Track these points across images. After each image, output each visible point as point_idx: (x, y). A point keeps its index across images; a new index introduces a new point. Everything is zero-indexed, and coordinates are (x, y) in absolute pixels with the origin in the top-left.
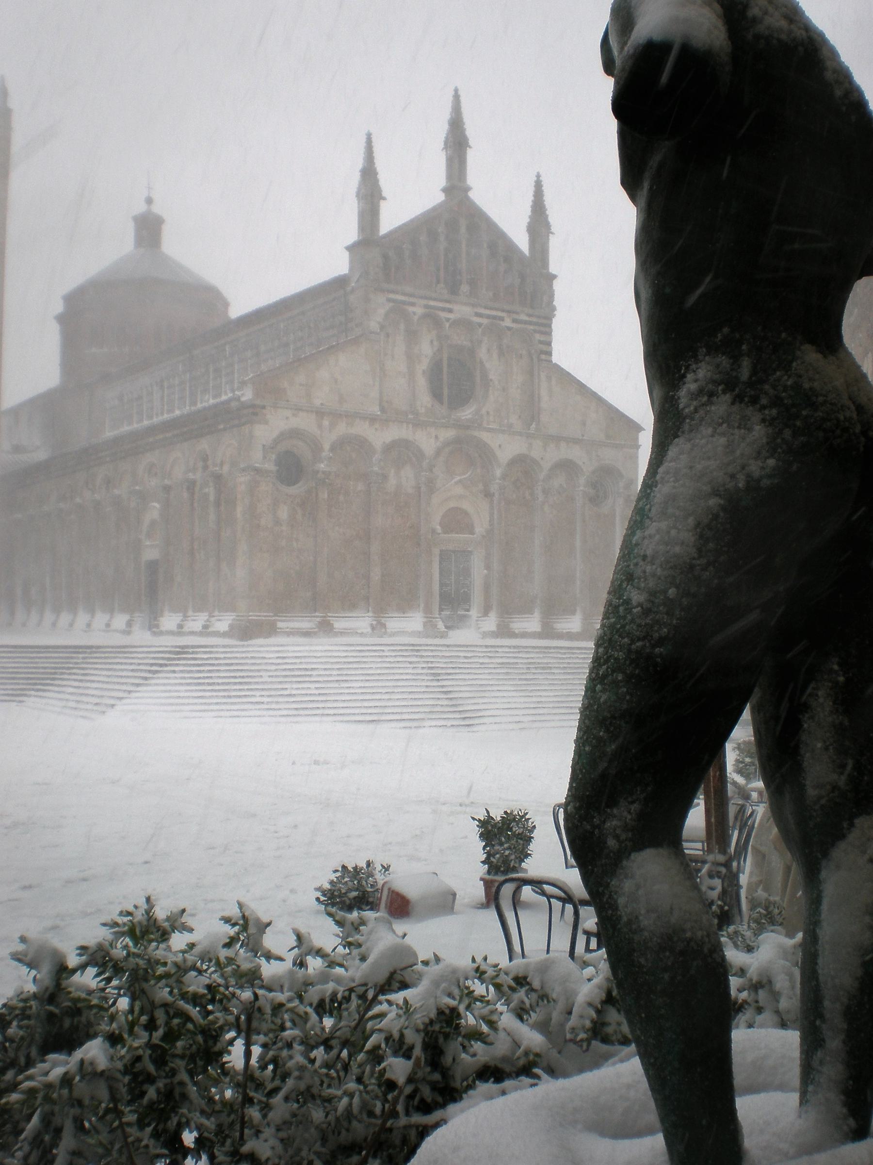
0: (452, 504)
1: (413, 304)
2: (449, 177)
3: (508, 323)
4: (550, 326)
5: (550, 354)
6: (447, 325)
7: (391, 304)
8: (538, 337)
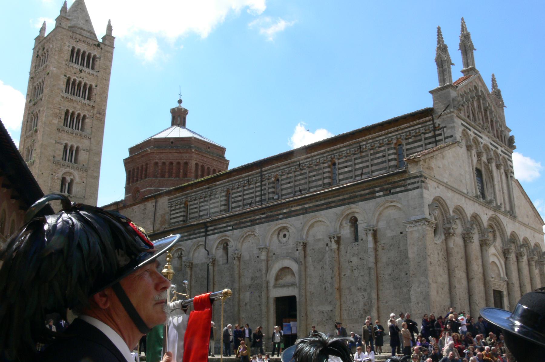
1: (470, 130)
2: (466, 64)
3: (499, 152)
4: (511, 157)
6: (482, 145)
7: (463, 127)
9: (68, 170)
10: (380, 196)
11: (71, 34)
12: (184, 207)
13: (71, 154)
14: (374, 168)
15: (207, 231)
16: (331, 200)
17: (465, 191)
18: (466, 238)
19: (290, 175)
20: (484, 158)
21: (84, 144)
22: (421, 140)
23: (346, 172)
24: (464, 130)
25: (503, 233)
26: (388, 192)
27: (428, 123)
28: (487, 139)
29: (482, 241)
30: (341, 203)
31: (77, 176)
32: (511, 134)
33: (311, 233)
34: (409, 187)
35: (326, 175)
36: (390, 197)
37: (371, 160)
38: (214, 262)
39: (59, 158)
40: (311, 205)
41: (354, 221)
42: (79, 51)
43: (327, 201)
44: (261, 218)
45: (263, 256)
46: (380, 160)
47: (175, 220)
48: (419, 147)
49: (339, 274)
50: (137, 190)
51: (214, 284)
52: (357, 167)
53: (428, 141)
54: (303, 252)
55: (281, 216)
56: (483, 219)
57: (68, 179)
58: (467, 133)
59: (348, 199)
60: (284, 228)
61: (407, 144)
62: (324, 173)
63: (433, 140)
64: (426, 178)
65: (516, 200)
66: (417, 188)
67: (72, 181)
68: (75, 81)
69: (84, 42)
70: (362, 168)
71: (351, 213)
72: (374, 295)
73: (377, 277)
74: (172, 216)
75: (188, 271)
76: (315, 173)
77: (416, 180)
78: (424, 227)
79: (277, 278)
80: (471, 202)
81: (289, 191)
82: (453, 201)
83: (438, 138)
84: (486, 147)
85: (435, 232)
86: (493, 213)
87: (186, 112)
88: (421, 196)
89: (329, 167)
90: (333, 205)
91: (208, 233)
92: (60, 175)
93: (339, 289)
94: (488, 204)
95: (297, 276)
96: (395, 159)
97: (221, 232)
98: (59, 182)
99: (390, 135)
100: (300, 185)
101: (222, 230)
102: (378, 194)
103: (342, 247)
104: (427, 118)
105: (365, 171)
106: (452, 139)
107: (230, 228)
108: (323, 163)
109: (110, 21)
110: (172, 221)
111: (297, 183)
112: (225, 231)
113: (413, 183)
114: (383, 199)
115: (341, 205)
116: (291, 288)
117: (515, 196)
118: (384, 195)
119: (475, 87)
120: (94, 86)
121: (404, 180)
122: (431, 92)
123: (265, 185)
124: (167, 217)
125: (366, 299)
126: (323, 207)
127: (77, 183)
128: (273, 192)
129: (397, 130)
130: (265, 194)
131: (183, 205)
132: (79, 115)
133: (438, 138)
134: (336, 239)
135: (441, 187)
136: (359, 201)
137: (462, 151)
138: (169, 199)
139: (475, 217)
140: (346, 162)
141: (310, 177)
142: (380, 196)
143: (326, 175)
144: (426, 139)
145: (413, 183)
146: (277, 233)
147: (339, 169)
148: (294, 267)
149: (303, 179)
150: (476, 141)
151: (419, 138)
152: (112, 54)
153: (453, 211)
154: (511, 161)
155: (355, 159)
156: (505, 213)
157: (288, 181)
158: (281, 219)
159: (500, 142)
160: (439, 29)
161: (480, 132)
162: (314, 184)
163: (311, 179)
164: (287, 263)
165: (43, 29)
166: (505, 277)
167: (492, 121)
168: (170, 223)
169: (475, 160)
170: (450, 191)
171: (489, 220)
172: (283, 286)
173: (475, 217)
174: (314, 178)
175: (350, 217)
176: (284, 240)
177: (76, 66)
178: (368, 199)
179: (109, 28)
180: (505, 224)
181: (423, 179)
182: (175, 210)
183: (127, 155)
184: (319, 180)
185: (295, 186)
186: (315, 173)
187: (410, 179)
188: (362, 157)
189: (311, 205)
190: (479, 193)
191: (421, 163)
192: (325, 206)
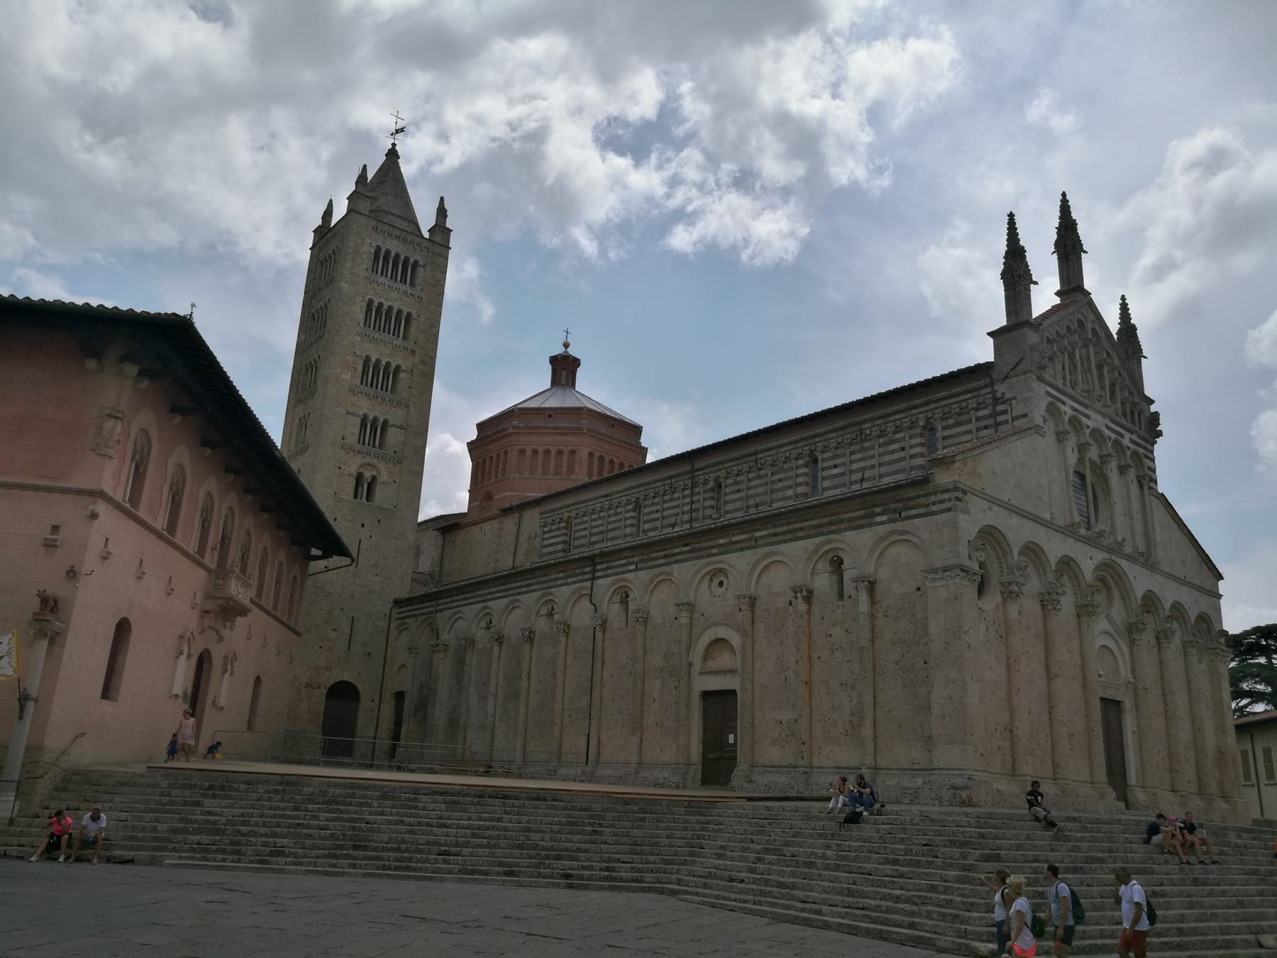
0: (1103, 641)
1: (1064, 403)
3: (1126, 442)
4: (1152, 452)
5: (1156, 482)
8: (1147, 462)
9: (368, 460)
10: (882, 523)
11: (373, 223)
12: (566, 528)
13: (373, 430)
14: (883, 470)
15: (594, 571)
16: (798, 525)
17: (1047, 516)
18: (1048, 602)
19: (739, 478)
20: (1093, 453)
21: (395, 415)
22: (969, 422)
23: (835, 476)
24: (1051, 404)
25: (1126, 594)
26: (898, 515)
27: (983, 392)
28: (1099, 418)
29: (1080, 607)
30: (813, 532)
31: (384, 472)
32: (1153, 408)
33: (764, 580)
34: (934, 508)
35: (801, 480)
36: (899, 526)
37: (880, 455)
38: (604, 625)
39: (352, 439)
40: (765, 533)
41: (837, 564)
42: (388, 252)
43: (792, 527)
44: (682, 553)
45: (684, 620)
46: (895, 456)
47: (551, 549)
48: (965, 433)
49: (810, 656)
50: (489, 496)
51: (603, 663)
52: (855, 466)
53: (982, 423)
54: (749, 614)
55: (715, 551)
56: (1083, 567)
57: (368, 475)
58: (1058, 409)
59: (827, 524)
60: (720, 570)
61: (944, 429)
62: (797, 476)
63: (990, 422)
64: (965, 492)
65: (1158, 531)
66: (949, 510)
67: (374, 478)
68: (381, 304)
69: (397, 237)
70: (863, 469)
71: (831, 550)
72: (868, 698)
73: (874, 665)
74: (545, 543)
75: (563, 639)
76: (781, 476)
77: (946, 496)
78: (957, 580)
79: (707, 655)
80: (1059, 536)
81: (738, 505)
82: (1018, 532)
83: (1000, 418)
84: (1097, 434)
85: (981, 590)
86: (1107, 556)
87: (576, 362)
88: (955, 525)
89: (806, 465)
90: (801, 534)
91: (597, 574)
92: (354, 470)
93: (808, 683)
94: (1094, 541)
95: (739, 656)
96: (923, 455)
97: (617, 574)
98: (353, 481)
99: (914, 412)
100: (756, 495)
101: (620, 570)
102: (878, 519)
103: (815, 608)
104: (981, 383)
105: (868, 474)
106: (1025, 420)
107: (633, 567)
108: (797, 459)
109: (442, 199)
110: (545, 550)
111: (751, 492)
112: (623, 573)
113: (941, 502)
114: (887, 528)
115: (816, 536)
116: (729, 676)
117: (1156, 525)
118: (891, 521)
119: (1080, 322)
120: (414, 315)
121: (925, 495)
122: (989, 334)
123: (699, 493)
124: (537, 543)
125: (854, 702)
126: (784, 538)
127: (386, 483)
128: (712, 507)
129: (927, 403)
130: (697, 510)
131: (562, 525)
132: (388, 364)
133: (1000, 418)
134: (804, 593)
135: (995, 508)
136: (846, 530)
137: (1046, 443)
138: (542, 514)
139: (1067, 564)
140: (835, 457)
141: (773, 482)
142: (882, 523)
143: (801, 480)
144: (978, 419)
145: (941, 502)
146: (707, 579)
147: (823, 469)
148: (735, 639)
149: (761, 485)
150: (1074, 422)
151: (964, 418)
152: (447, 258)
153: (1021, 553)
154: (1153, 460)
155: (852, 453)
156: (1131, 558)
157: (737, 487)
158: (714, 555)
159: (1129, 425)
160: (1011, 216)
161: (1086, 407)
162: (780, 495)
163: (774, 486)
164: (722, 632)
165: (328, 213)
166: (1130, 675)
167: (1112, 385)
168: (543, 555)
169: (1073, 458)
170: (1015, 517)
171: (1097, 568)
172: (716, 673)
173: (1067, 564)
174: (780, 485)
175: (830, 556)
176: (720, 590)
177: (382, 279)
178: (862, 527)
179: (442, 212)
180: (1131, 577)
181: (960, 495)
182: (550, 531)
183: (473, 435)
184: (789, 487)
185: (748, 497)
186: (781, 476)
187: (935, 493)
188: (863, 449)
189: (765, 533)
190: (1077, 519)
191: (957, 465)
192: (789, 536)
